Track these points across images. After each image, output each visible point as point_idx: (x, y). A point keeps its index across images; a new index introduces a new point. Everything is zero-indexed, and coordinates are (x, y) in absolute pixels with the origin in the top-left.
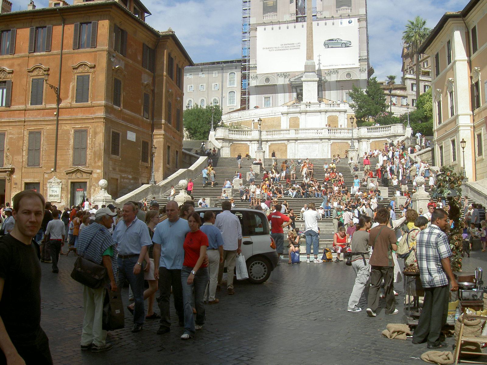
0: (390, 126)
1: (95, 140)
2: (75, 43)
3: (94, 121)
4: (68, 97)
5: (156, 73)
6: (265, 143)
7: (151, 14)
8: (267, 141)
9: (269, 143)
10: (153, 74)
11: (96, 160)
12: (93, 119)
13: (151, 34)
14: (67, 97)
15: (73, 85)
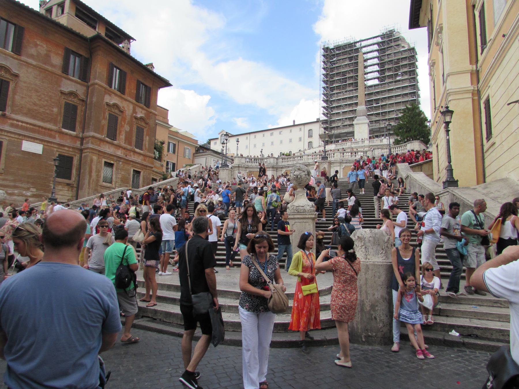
0: (406, 145)
6: (280, 170)
7: (135, 40)
8: (282, 168)
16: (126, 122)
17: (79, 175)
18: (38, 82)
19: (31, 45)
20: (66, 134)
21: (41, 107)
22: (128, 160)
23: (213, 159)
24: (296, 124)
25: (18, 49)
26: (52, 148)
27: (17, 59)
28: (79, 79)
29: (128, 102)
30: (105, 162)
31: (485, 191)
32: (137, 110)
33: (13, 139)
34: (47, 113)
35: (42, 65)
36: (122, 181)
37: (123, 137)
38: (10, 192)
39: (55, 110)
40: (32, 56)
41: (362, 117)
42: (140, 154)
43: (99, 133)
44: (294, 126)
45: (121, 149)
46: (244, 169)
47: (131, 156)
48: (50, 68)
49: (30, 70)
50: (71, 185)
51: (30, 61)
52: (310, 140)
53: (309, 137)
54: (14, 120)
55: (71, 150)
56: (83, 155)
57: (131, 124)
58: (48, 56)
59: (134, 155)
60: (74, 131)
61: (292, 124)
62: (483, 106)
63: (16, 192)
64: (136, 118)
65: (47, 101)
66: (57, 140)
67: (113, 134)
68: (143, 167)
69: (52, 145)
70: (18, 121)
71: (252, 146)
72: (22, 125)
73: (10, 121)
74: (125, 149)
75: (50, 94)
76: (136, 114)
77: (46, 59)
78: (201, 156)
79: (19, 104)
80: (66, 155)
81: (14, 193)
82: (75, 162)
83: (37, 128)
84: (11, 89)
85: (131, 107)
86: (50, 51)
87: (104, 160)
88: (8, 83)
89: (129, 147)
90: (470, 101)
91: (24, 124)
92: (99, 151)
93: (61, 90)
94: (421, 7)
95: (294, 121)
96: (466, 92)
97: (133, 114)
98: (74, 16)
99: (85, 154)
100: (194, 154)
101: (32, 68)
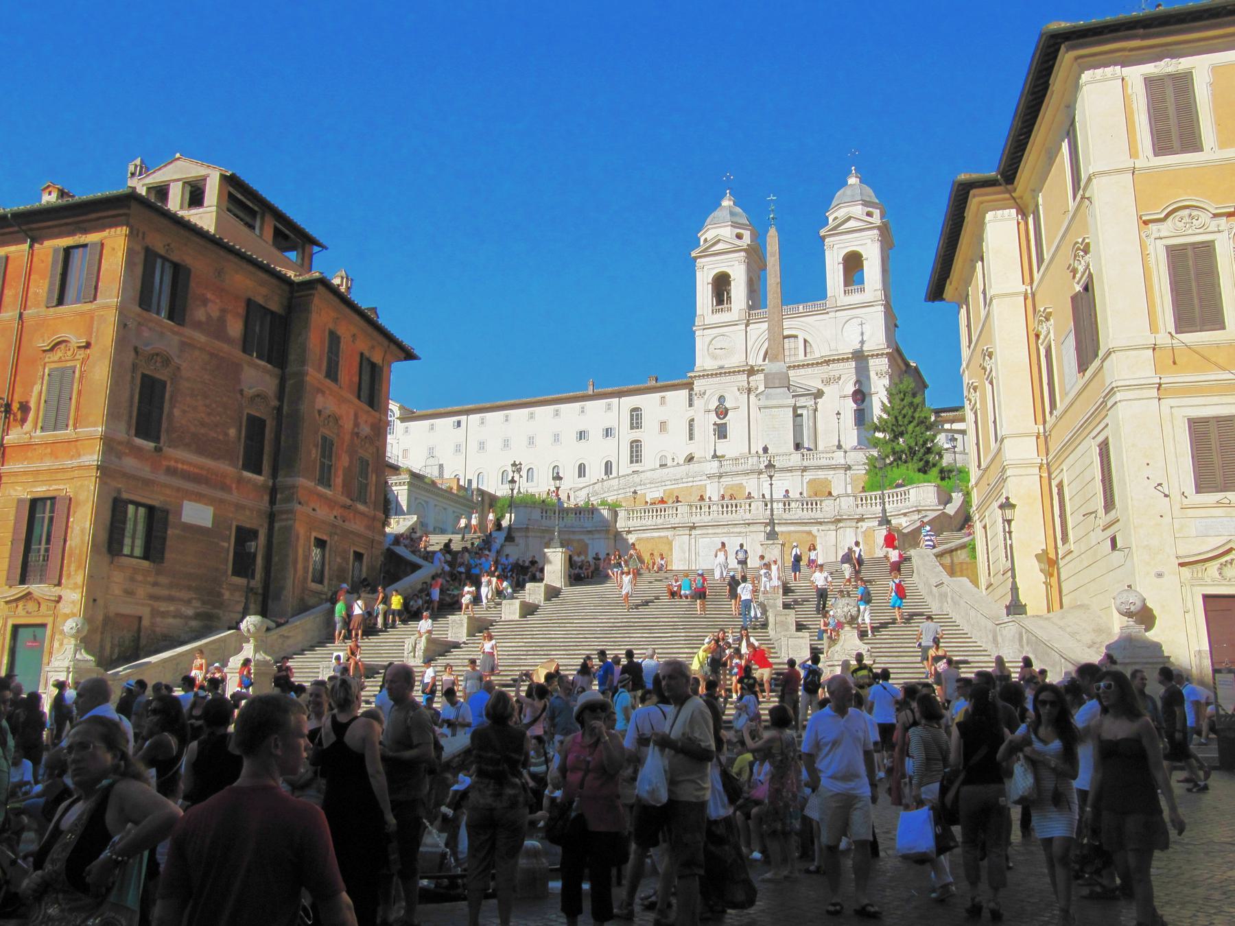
1: (73, 522)
3: (76, 473)
5: (287, 370)
7: (326, 249)
10: (277, 371)
13: (274, 281)
20: (249, 480)
25: (177, 313)
28: (269, 362)
37: (339, 481)
39: (232, 432)
40: (198, 325)
41: (779, 390)
42: (362, 514)
46: (539, 534)
56: (277, 525)
58: (222, 321)
60: (259, 473)
62: (1055, 490)
66: (234, 497)
67: (325, 480)
70: (177, 461)
72: (182, 469)
73: (165, 463)
87: (314, 534)
94: (949, 277)
96: (1032, 465)
97: (353, 429)
98: (225, 210)
99: (283, 524)
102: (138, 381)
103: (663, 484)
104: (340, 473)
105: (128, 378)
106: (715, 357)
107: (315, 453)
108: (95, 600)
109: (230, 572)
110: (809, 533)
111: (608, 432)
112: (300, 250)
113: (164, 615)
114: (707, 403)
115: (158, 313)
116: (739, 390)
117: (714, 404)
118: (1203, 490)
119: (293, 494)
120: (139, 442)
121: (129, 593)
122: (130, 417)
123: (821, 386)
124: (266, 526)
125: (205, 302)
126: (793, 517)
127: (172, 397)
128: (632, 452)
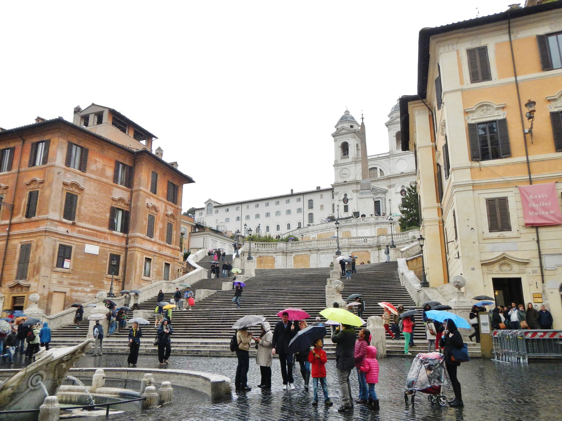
0: (408, 232)
2: (30, 161)
3: (38, 234)
4: (20, 212)
6: (290, 254)
7: (158, 138)
9: (294, 255)
11: (35, 273)
12: (36, 232)
14: (18, 214)
15: (25, 201)
16: (160, 221)
17: (124, 271)
18: (97, 193)
19: (93, 163)
21: (98, 214)
22: (161, 254)
23: (211, 239)
24: (294, 192)
25: (83, 167)
26: (106, 249)
27: (83, 176)
28: (125, 186)
29: (162, 202)
30: (146, 258)
31: (441, 291)
32: (168, 209)
33: (79, 243)
34: (103, 219)
35: (99, 178)
36: (157, 274)
38: (75, 289)
40: (92, 172)
43: (142, 233)
44: (292, 195)
45: (156, 245)
47: (163, 250)
48: (104, 180)
49: (92, 183)
50: (119, 280)
51: (92, 176)
52: (311, 211)
53: (309, 208)
54: (80, 227)
55: (119, 249)
56: (128, 253)
57: (163, 222)
58: (103, 170)
59: (165, 249)
61: (289, 193)
63: (80, 289)
64: (167, 215)
65: (102, 208)
66: (109, 241)
67: (151, 233)
68: (171, 259)
69: (106, 246)
70: (83, 228)
71: (244, 217)
73: (77, 229)
74: (159, 244)
75: (105, 202)
76: (167, 212)
77: (102, 173)
78: (197, 235)
79: (83, 213)
80: (115, 253)
81: (78, 290)
82: (122, 259)
83: (95, 232)
84: (78, 201)
85: (164, 205)
86: (105, 165)
87: (145, 256)
88: (77, 196)
89: (162, 243)
90: (438, 227)
91: (86, 230)
92: (142, 249)
93: (112, 198)
94: (409, 140)
95: (292, 191)
99: (131, 252)
100: (190, 233)
101: (93, 181)
102: (65, 196)
103: (317, 231)
104: (158, 231)
105: (60, 194)
106: (342, 178)
107: (146, 223)
108: (44, 286)
109: (107, 273)
110: (367, 251)
111: (299, 210)
112: (147, 141)
113: (76, 291)
114: (339, 197)
115: (74, 167)
116: (353, 191)
117: (342, 197)
118: (492, 231)
119: (135, 240)
120: (65, 220)
121: (60, 283)
122: (61, 211)
123: (387, 188)
124: (124, 253)
125: (96, 162)
126: (360, 245)
127: (80, 201)
128: (309, 218)
